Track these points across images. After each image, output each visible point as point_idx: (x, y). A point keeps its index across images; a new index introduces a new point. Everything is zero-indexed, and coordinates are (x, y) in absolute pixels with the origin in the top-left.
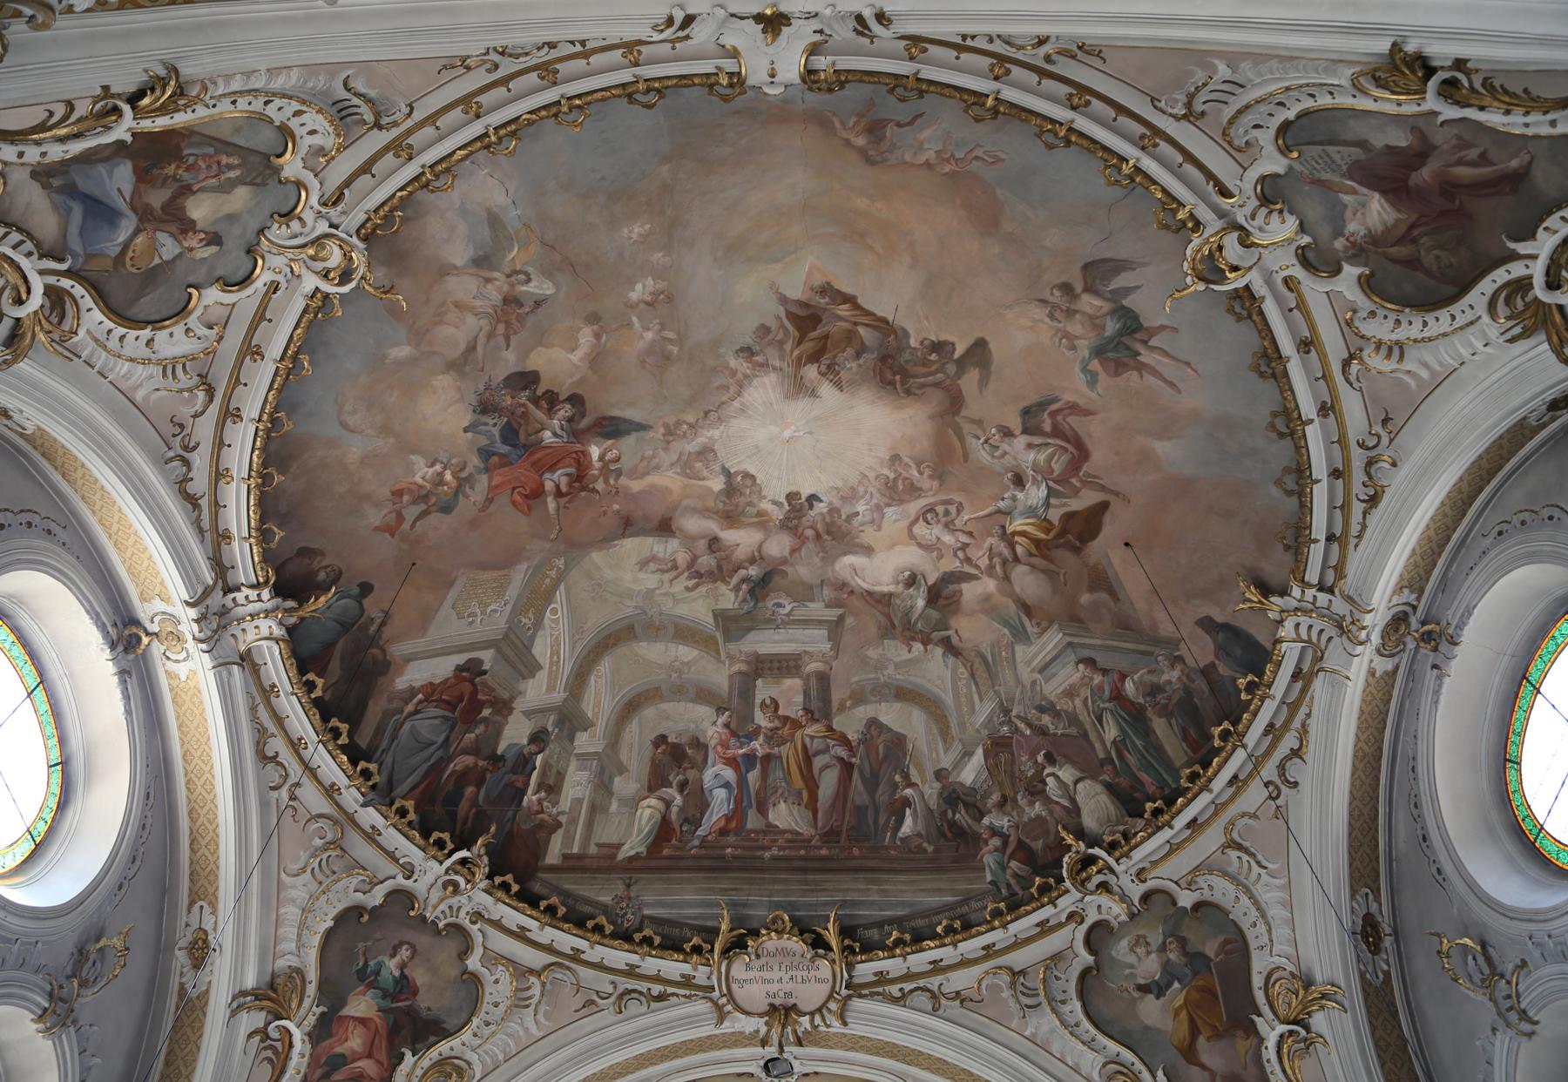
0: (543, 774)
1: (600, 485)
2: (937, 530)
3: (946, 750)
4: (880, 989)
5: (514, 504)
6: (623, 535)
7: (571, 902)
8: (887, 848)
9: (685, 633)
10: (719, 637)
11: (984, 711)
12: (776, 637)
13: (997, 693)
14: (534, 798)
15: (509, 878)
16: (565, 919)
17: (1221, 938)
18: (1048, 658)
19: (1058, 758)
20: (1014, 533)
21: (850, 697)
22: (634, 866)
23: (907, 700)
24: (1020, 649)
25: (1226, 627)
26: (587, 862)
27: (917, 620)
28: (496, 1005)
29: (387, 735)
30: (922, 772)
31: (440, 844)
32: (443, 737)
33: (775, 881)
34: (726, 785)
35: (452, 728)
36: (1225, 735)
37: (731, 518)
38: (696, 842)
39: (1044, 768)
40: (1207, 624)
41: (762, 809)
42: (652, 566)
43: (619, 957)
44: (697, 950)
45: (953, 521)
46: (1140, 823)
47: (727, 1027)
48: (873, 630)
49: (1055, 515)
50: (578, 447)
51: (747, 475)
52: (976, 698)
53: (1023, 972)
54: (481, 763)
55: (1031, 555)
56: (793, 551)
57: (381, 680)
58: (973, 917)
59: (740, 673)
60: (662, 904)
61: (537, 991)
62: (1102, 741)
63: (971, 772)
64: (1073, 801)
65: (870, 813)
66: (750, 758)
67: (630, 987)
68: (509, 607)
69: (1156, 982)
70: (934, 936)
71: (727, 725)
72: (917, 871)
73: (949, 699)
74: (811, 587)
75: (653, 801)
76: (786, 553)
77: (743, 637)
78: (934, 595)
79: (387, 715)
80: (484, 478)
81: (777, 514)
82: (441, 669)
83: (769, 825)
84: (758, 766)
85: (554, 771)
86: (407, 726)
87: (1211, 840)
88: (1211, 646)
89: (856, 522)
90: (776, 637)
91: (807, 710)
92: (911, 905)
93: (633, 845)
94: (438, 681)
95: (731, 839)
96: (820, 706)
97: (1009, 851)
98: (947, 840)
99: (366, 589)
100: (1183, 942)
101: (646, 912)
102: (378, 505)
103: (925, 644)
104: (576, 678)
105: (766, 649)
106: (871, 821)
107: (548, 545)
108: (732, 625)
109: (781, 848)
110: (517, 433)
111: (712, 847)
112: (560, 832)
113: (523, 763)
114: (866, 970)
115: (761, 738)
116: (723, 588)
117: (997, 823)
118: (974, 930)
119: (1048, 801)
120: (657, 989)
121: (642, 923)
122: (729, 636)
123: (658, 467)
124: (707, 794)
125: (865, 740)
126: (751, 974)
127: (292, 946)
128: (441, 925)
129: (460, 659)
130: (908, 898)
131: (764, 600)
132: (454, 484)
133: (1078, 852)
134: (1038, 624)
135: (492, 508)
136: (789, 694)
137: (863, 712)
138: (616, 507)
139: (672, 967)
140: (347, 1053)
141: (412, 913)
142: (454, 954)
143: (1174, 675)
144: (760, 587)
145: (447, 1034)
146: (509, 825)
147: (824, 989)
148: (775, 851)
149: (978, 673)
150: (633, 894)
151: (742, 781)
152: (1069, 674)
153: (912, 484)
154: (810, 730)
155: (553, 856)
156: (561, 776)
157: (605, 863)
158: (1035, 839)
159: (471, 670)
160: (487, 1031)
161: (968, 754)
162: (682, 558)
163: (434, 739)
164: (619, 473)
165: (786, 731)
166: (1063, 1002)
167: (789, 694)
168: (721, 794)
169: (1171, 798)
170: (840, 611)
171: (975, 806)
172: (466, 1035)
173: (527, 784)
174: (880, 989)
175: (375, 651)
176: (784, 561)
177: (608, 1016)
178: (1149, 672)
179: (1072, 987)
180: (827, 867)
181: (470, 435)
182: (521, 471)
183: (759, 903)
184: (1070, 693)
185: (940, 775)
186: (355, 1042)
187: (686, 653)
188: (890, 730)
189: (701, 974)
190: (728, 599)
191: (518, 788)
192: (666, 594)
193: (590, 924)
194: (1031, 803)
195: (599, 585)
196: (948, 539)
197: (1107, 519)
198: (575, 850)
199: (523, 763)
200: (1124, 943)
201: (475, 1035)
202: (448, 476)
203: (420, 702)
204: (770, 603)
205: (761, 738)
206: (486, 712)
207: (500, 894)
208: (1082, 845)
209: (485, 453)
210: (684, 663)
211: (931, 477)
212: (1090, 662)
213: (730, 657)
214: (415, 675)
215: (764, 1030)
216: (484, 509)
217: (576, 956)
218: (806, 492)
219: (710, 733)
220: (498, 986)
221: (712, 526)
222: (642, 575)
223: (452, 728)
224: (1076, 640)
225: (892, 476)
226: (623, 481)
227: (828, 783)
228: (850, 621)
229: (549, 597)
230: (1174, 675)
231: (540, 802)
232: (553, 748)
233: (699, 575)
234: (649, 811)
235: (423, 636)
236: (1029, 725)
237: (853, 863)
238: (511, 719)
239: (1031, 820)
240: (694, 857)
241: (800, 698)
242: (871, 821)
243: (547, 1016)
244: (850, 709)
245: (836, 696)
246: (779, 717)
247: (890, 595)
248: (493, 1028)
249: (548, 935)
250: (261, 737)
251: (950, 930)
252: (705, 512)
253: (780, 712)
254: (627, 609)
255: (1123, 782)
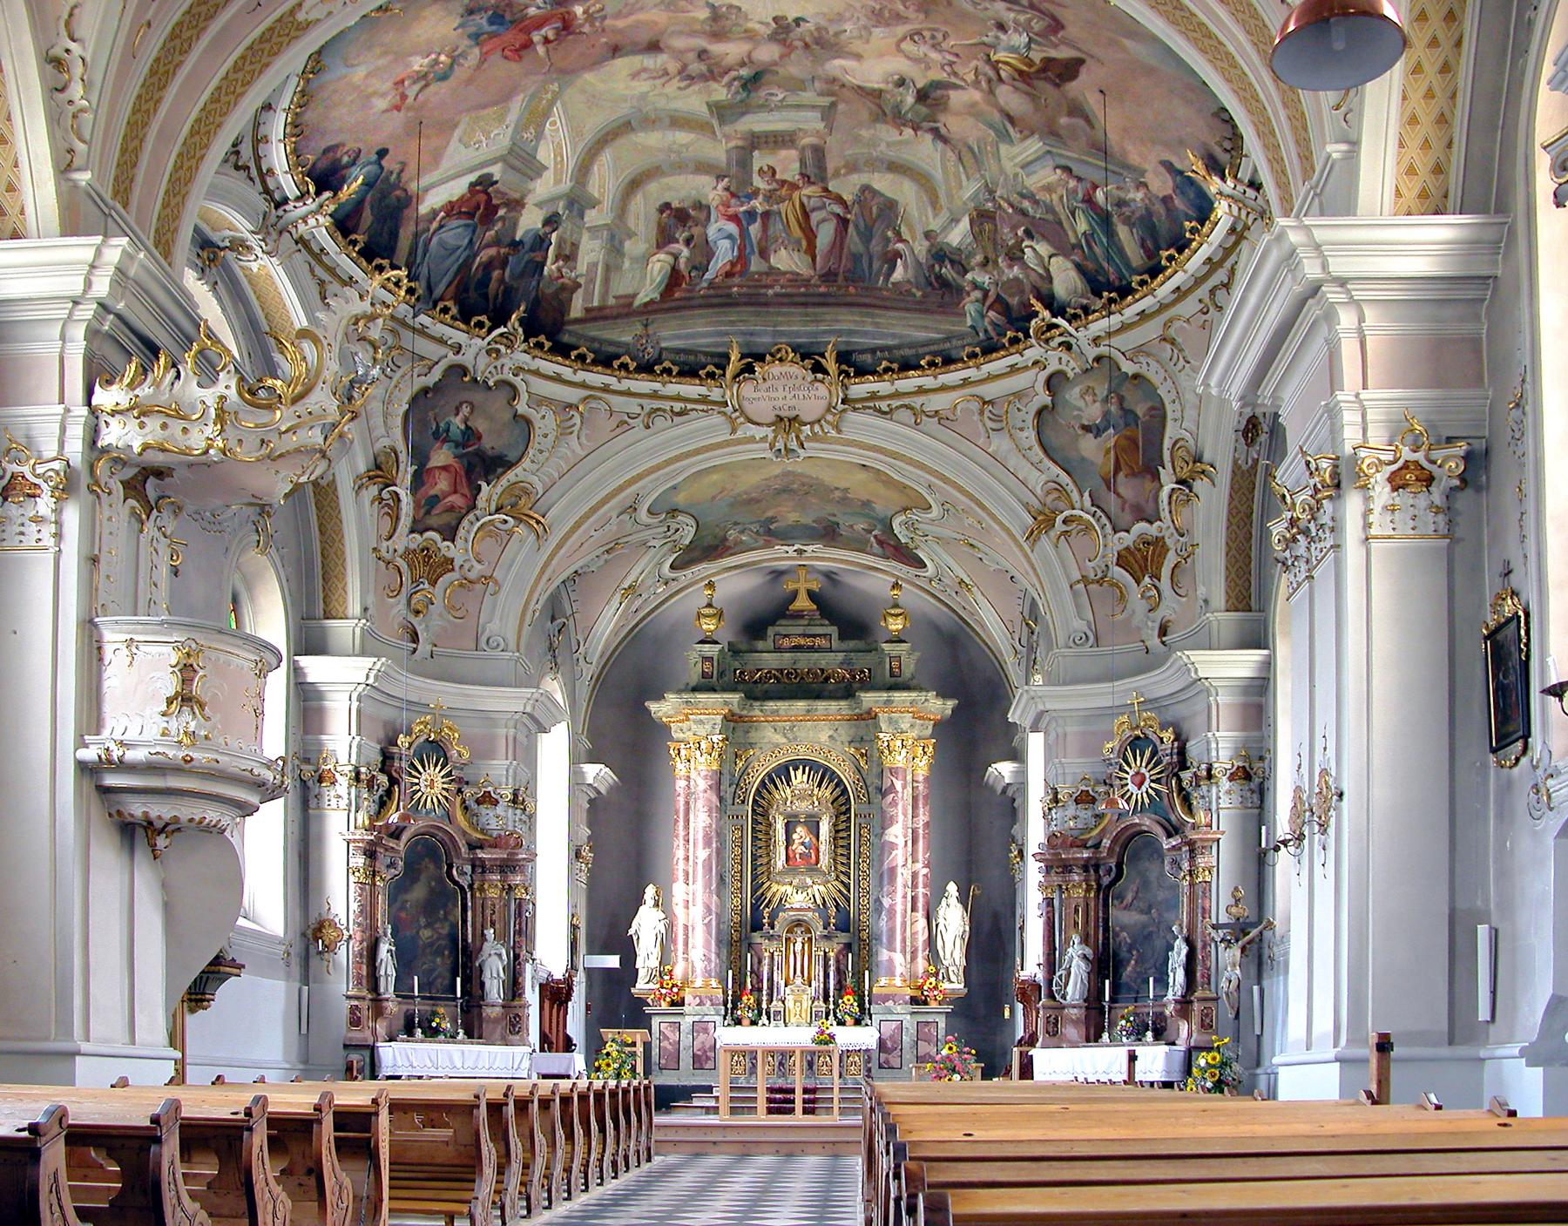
0: (559, 246)
1: (586, 29)
2: (923, 49)
3: (935, 216)
4: (872, 404)
5: (506, 58)
6: (613, 57)
7: (596, 345)
8: (881, 289)
9: (678, 122)
10: (715, 123)
11: (970, 189)
12: (771, 118)
13: (983, 176)
14: (553, 267)
15: (542, 338)
16: (595, 362)
17: (1149, 404)
18: (1030, 159)
19: (1036, 236)
20: (998, 62)
21: (844, 167)
22: (649, 309)
23: (899, 173)
24: (1003, 148)
25: (1181, 173)
26: (607, 312)
27: (907, 112)
28: (546, 436)
29: (420, 252)
30: (911, 229)
31: (480, 325)
32: (466, 241)
33: (779, 314)
34: (730, 237)
35: (474, 232)
36: (1170, 259)
37: (718, 35)
38: (705, 284)
39: (1023, 241)
40: (1168, 166)
41: (764, 254)
42: (644, 75)
43: (643, 385)
44: (711, 375)
45: (939, 44)
46: (1098, 304)
47: (739, 434)
48: (865, 115)
49: (1037, 56)
50: (563, 10)
51: (730, 6)
52: (963, 177)
53: (989, 402)
54: (502, 251)
55: (1014, 79)
56: (782, 57)
57: (406, 212)
58: (954, 354)
59: (737, 147)
60: (678, 337)
61: (577, 420)
62: (1075, 232)
63: (958, 235)
64: (1048, 271)
65: (865, 260)
66: (751, 215)
67: (655, 407)
68: (510, 130)
69: (1096, 425)
70: (917, 367)
71: (727, 189)
72: (907, 310)
73: (938, 174)
74: (803, 82)
75: (662, 256)
76: (776, 56)
77: (736, 120)
78: (922, 96)
79: (417, 236)
80: (477, 51)
81: (766, 31)
82: (457, 189)
83: (771, 268)
84: (759, 220)
85: (569, 244)
86: (435, 240)
87: (1152, 329)
88: (1170, 183)
89: (843, 37)
90: (771, 118)
91: (803, 175)
92: (901, 337)
93: (648, 292)
94: (455, 199)
95: (736, 280)
96: (816, 168)
97: (988, 303)
98: (934, 289)
99: (382, 153)
100: (1121, 400)
101: (664, 345)
102: (384, 95)
103: (915, 130)
104: (580, 170)
105: (759, 127)
106: (865, 266)
107: (542, 77)
108: (722, 112)
109: (782, 287)
110: (503, 17)
111: (719, 287)
112: (580, 291)
113: (541, 242)
114: (860, 389)
115: (761, 198)
116: (714, 85)
117: (979, 279)
118: (952, 367)
119: (1025, 266)
120: (678, 406)
121: (660, 355)
122: (722, 120)
123: (642, 8)
124: (711, 244)
125: (859, 201)
126: (758, 395)
127: (382, 431)
128: (491, 383)
129: (473, 177)
130: (897, 330)
131: (757, 89)
132: (449, 61)
133: (1043, 320)
134: (1021, 132)
135: (486, 65)
136: (788, 164)
137: (857, 180)
138: (604, 40)
139: (691, 389)
140: (439, 494)
141: (466, 379)
142: (505, 402)
143: (1139, 196)
144: (754, 81)
145: (510, 465)
146: (534, 294)
147: (824, 403)
148: (777, 289)
149: (965, 160)
150: (650, 332)
151: (744, 233)
152: (1045, 175)
153: (898, 15)
154: (808, 191)
155: (577, 309)
156: (575, 246)
157: (625, 310)
158: (1012, 295)
159: (485, 183)
160: (541, 458)
161: (955, 220)
162: (673, 67)
163: (459, 243)
164: (604, 18)
165: (784, 192)
166: (1022, 429)
167: (788, 164)
168: (726, 244)
169: (1125, 291)
170: (833, 99)
171: (960, 263)
172: (526, 463)
173: (546, 258)
174: (872, 404)
175: (398, 192)
176: (775, 64)
177: (639, 431)
178: (1118, 188)
179: (1030, 418)
180: (824, 302)
181: (460, 30)
182: (512, 37)
183: (763, 331)
184: (1049, 189)
185: (928, 235)
186: (443, 484)
187: (682, 137)
188: (883, 195)
189: (716, 394)
190: (720, 93)
191: (538, 263)
192: (660, 95)
193: (616, 364)
194: (1011, 267)
195: (594, 96)
196: (934, 55)
197: (1083, 71)
198: (596, 304)
199: (541, 242)
200: (1077, 391)
201: (533, 462)
202: (443, 58)
203: (443, 218)
204: (762, 93)
205: (761, 198)
206: (501, 212)
207: (537, 352)
208: (1046, 314)
209: (476, 37)
210: (682, 145)
211: (918, 11)
212: (1067, 170)
213: (725, 136)
214: (434, 200)
215: (771, 436)
216: (478, 68)
217: (606, 389)
218: (791, 16)
219: (711, 197)
220: (545, 423)
221: (701, 43)
222: (635, 84)
223: (474, 232)
224: (1054, 150)
225: (878, 7)
226: (608, 22)
227: (825, 235)
228: (841, 107)
229: (547, 114)
230: (1139, 196)
231: (559, 270)
232: (566, 226)
233: (691, 78)
234: (659, 265)
235: (437, 169)
236: (1012, 206)
237: (849, 299)
238: (524, 212)
239: (1008, 279)
240: (702, 297)
241: (797, 165)
242: (865, 266)
243: (588, 437)
244: (845, 175)
245: (831, 164)
246: (777, 181)
247: (881, 91)
248: (546, 454)
249: (582, 376)
250: (322, 283)
251: (932, 364)
252: (693, 33)
253: (777, 177)
254: (624, 110)
255: (1090, 265)
